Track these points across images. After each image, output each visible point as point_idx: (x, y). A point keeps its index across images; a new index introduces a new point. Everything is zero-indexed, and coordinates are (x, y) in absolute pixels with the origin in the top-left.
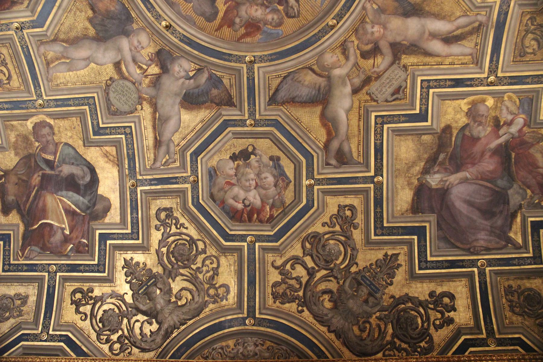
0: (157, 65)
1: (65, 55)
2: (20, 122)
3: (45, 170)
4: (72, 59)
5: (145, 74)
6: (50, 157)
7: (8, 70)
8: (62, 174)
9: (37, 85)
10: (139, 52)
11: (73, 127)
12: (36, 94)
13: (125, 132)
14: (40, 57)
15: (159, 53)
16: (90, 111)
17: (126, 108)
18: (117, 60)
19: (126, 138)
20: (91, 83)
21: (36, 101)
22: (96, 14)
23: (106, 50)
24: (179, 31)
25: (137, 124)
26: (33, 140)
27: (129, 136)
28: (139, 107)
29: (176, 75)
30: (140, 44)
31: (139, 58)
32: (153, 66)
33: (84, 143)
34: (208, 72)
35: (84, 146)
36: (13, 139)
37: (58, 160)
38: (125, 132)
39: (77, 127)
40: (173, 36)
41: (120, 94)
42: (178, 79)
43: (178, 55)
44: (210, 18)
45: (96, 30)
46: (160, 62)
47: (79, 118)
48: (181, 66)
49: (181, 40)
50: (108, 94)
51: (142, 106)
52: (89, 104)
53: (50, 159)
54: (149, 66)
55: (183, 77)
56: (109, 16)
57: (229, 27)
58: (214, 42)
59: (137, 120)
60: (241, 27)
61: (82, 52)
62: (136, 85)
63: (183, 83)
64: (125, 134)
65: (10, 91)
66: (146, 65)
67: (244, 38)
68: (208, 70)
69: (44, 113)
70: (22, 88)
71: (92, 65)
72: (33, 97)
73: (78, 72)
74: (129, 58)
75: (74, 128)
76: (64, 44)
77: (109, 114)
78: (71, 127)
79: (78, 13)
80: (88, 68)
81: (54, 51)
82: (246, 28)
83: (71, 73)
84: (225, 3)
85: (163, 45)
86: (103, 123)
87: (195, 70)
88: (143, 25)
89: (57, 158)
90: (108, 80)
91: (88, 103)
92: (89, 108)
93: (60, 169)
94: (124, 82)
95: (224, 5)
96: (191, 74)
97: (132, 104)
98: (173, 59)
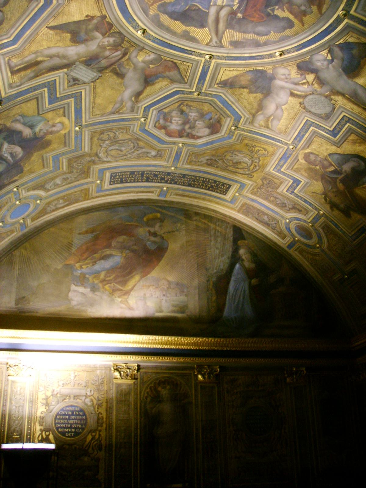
0: (308, 74)
1: (267, 116)
2: (297, 164)
3: (338, 177)
4: (273, 114)
5: (310, 84)
6: (332, 169)
7: (259, 147)
8: (347, 172)
9: (279, 141)
10: (290, 79)
11: (320, 143)
12: (284, 145)
13: (346, 121)
14: (261, 129)
15: (299, 67)
16: (316, 127)
17: (328, 109)
18: (289, 93)
19: (350, 123)
20: (296, 115)
21: (288, 148)
22: (248, 87)
23: (277, 95)
24: (290, 49)
25: (345, 111)
26: (314, 167)
27: (351, 121)
28: (333, 102)
29: (324, 67)
30: (285, 75)
31: (296, 81)
32: (307, 76)
33: (336, 146)
34: (336, 46)
35: (339, 147)
36: (306, 175)
37: (337, 166)
38: (346, 121)
39: (323, 142)
40: (291, 53)
41: (315, 106)
42: (328, 68)
43: (308, 57)
44: (291, 24)
45: (259, 93)
46: (307, 70)
47: (316, 137)
48: (319, 61)
49: (298, 50)
50: (310, 112)
51: (334, 100)
52: (310, 126)
53: (333, 169)
54: (305, 78)
55: (328, 64)
56: (254, 81)
57: (305, 16)
58: (312, 31)
59: (342, 109)
60: (310, 7)
61: (271, 107)
62: (315, 93)
63: (334, 67)
64: (347, 122)
65: (273, 154)
66: (303, 80)
67: (322, 10)
68: (333, 46)
69: (299, 150)
70: (275, 148)
71: (283, 107)
72: (285, 148)
73: (284, 117)
74: (292, 86)
75: (322, 143)
76: (259, 113)
77: (325, 120)
78: (319, 145)
79: (242, 96)
80: (284, 112)
81: (261, 120)
82: (314, 5)
83: (282, 121)
84: (284, 11)
85: (294, 62)
86: (330, 127)
87: (328, 53)
88: (272, 66)
89: (335, 166)
90: (300, 106)
91: (309, 125)
92: (313, 126)
93: (343, 171)
94: (308, 98)
95: (285, 12)
96: (329, 57)
97: (328, 104)
98: (310, 61)
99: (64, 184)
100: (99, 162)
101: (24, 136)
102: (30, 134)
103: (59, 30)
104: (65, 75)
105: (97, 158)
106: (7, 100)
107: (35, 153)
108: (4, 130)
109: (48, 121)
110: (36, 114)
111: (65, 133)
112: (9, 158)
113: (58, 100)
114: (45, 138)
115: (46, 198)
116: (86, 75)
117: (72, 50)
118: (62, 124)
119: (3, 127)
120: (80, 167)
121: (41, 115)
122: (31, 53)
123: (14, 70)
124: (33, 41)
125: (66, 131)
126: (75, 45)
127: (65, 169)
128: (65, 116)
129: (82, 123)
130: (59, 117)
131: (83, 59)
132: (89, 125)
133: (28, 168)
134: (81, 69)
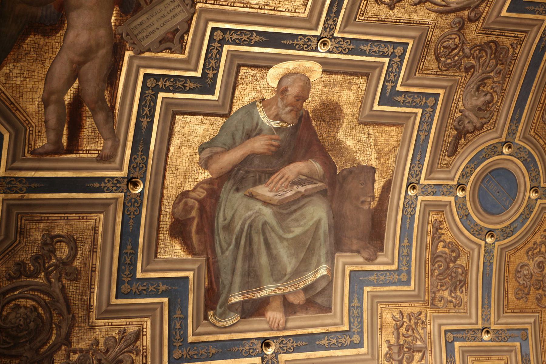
99: (498, 90)
100: (481, 9)
101: (265, 151)
102: (271, 139)
103: (8, 53)
104: (142, 55)
105: (466, 13)
106: (137, 169)
107: (335, 137)
108: (216, 187)
109: (263, 100)
110: (221, 121)
111: (324, 71)
112: (302, 189)
113: (211, 76)
114: (309, 111)
115: (512, 132)
116: (164, 16)
117: (78, 35)
118: (287, 75)
119: (206, 186)
120: (467, 51)
121: (233, 111)
122: (43, 112)
123: (65, 148)
124: (12, 103)
125: (318, 68)
126: (65, 29)
127: (445, 84)
128: (269, 68)
129: (315, 36)
130: (264, 77)
131: (113, 18)
132: (331, 22)
133: (374, 155)
134: (141, 24)
